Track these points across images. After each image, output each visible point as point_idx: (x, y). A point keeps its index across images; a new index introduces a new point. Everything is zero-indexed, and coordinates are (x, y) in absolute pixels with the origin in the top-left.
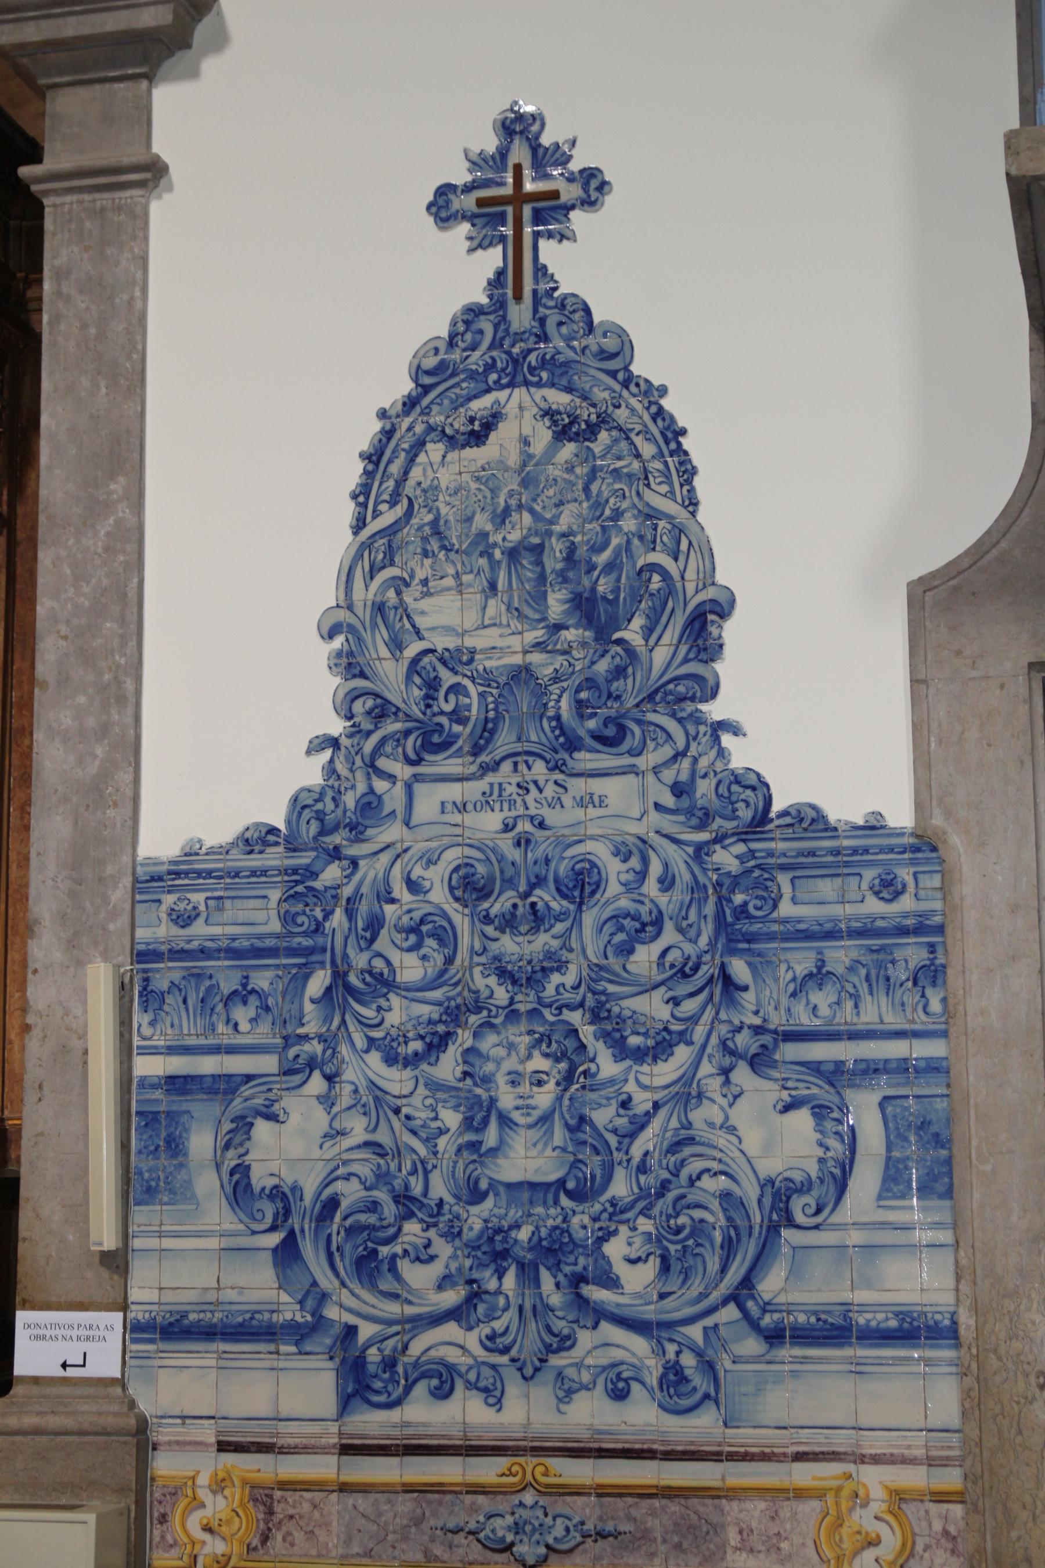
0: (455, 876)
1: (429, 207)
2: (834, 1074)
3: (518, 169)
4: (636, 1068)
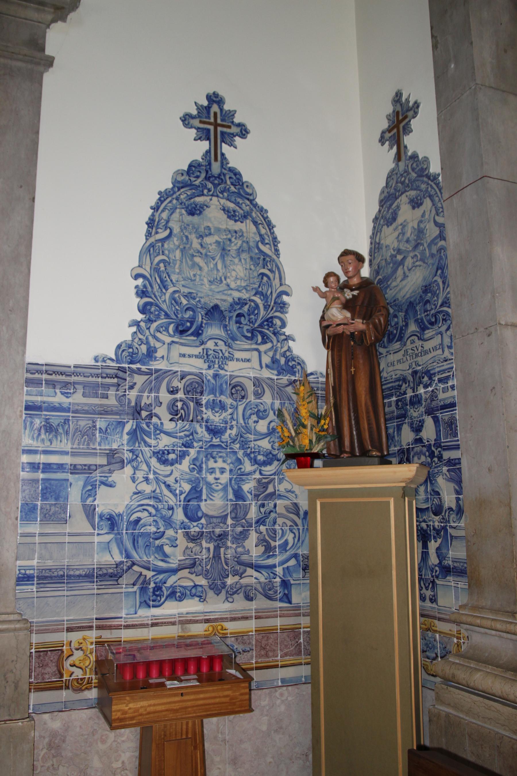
3: (215, 114)
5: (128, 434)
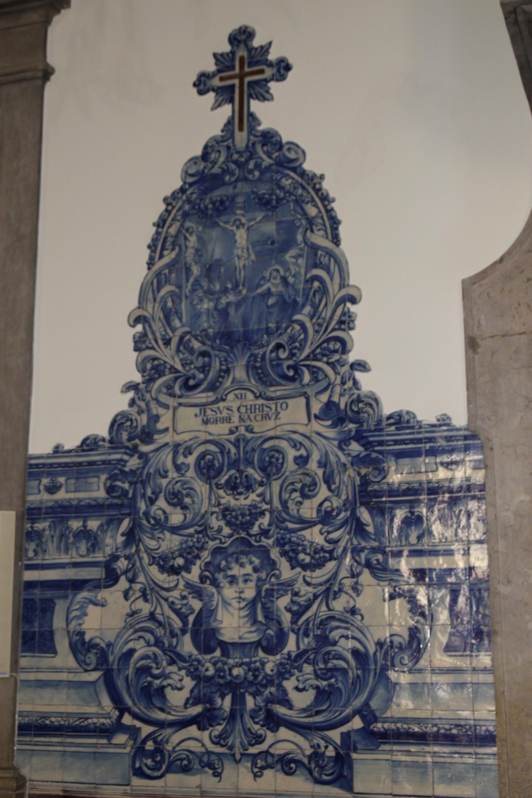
0: (202, 462)
1: (195, 85)
4: (303, 573)
5: (123, 535)
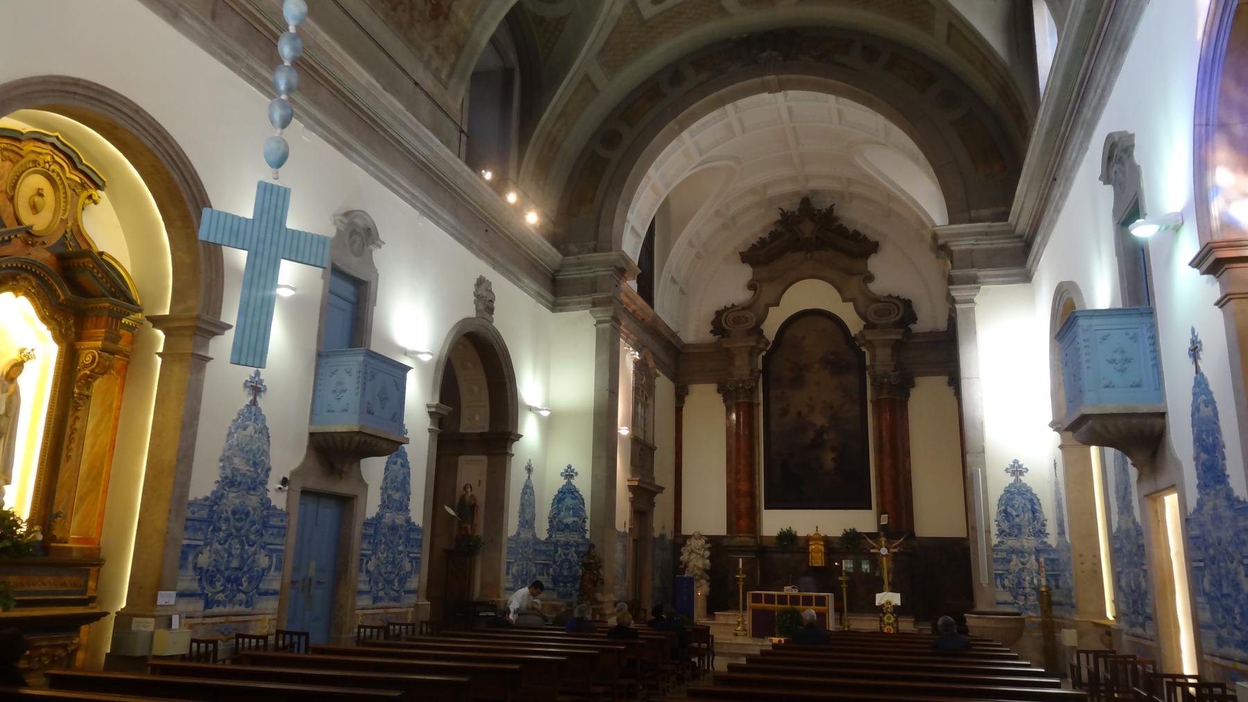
2: (272, 551)
